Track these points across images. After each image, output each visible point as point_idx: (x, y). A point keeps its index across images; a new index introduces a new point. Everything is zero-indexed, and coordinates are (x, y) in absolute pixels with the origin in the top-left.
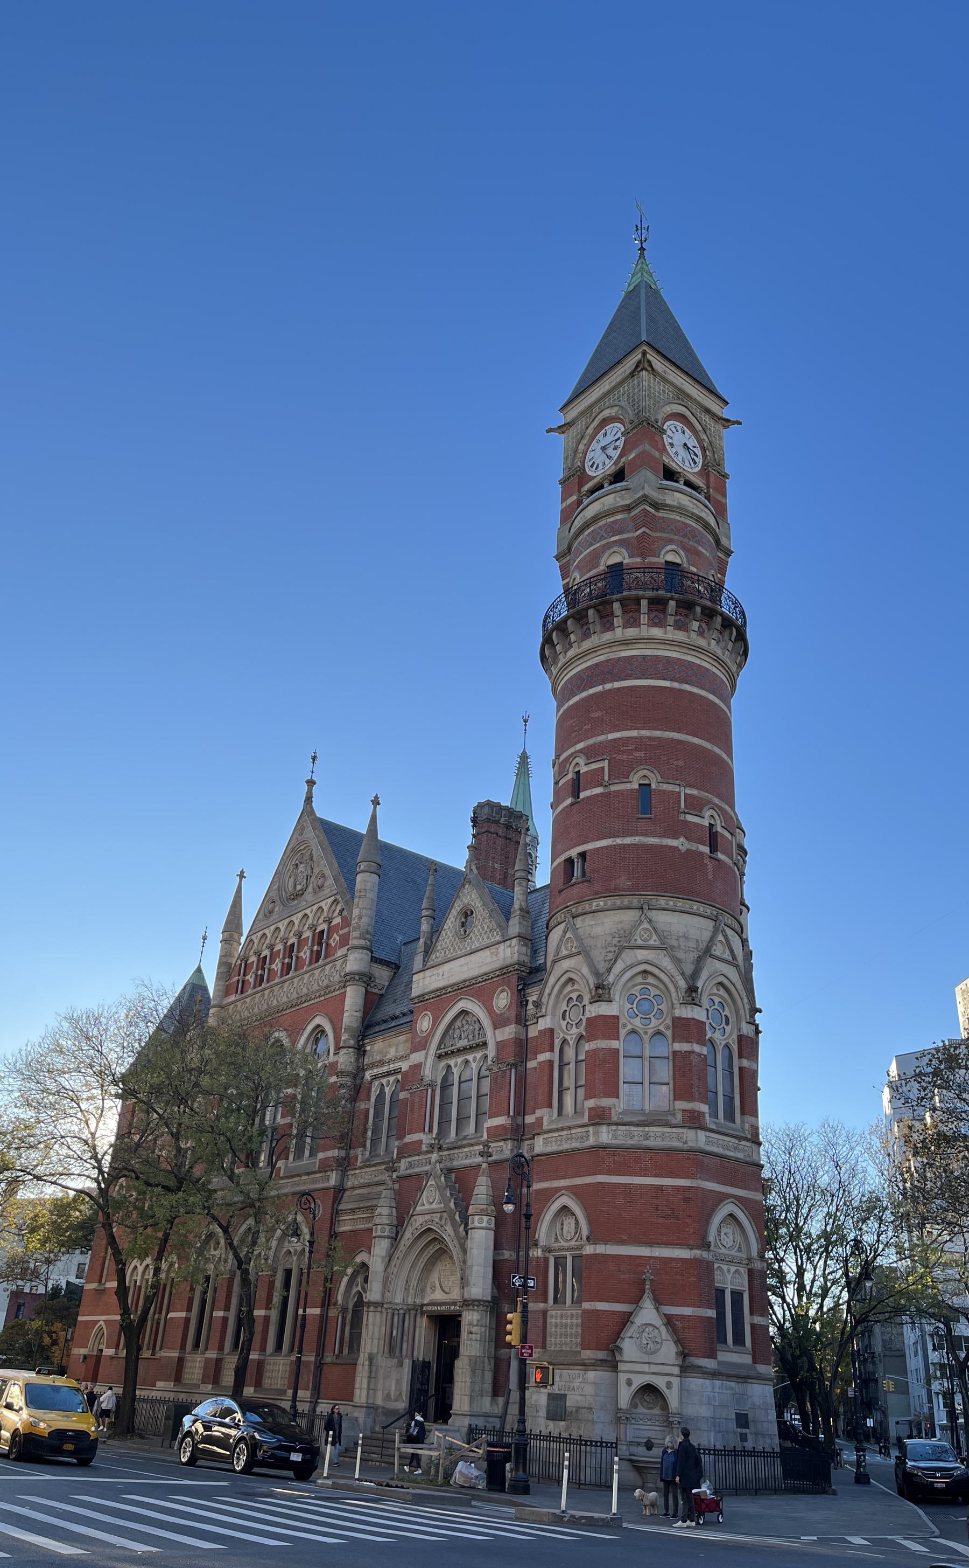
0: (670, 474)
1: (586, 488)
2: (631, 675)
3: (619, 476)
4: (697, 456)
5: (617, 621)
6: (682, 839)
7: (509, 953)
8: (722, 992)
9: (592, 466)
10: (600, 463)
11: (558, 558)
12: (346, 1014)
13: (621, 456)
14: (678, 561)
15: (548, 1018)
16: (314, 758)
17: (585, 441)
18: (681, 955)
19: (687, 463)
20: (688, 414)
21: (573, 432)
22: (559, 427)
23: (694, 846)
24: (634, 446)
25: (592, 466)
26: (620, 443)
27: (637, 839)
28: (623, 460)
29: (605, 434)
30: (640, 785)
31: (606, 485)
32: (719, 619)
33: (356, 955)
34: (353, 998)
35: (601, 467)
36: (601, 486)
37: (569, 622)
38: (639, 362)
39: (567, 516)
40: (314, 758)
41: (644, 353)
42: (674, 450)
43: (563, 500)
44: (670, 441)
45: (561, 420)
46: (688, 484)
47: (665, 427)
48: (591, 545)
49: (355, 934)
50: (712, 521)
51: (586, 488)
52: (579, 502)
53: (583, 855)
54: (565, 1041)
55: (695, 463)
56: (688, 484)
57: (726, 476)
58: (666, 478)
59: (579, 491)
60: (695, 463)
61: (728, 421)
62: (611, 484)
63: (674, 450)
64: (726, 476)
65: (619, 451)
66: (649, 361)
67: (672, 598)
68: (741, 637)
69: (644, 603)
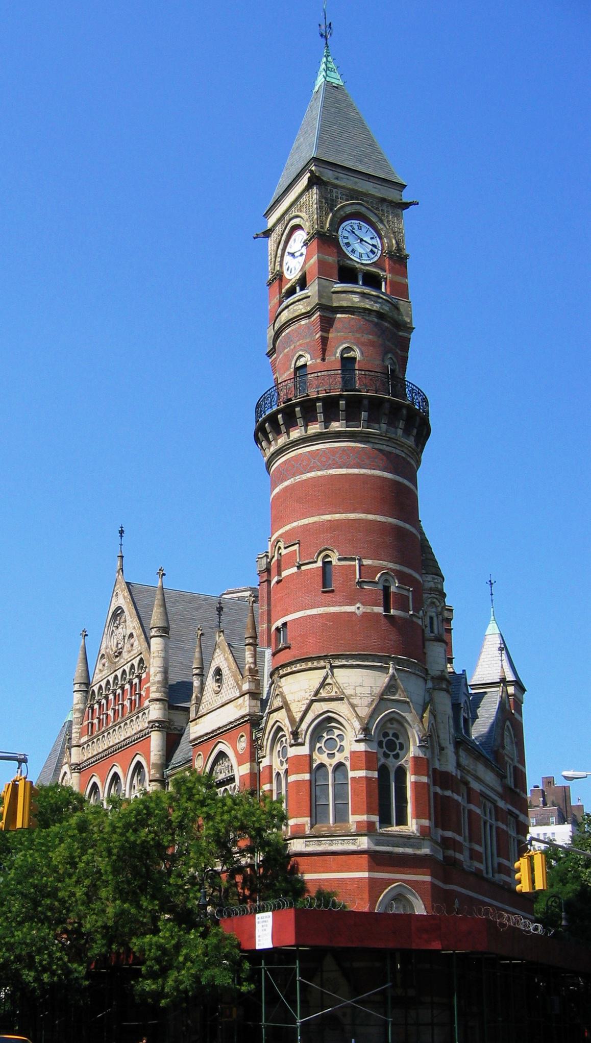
2: (314, 467)
6: (358, 605)
7: (244, 707)
8: (395, 725)
12: (152, 754)
13: (305, 263)
15: (268, 757)
16: (121, 532)
17: (281, 246)
18: (355, 701)
20: (363, 210)
23: (368, 609)
27: (322, 609)
30: (324, 563)
31: (298, 288)
33: (155, 706)
34: (156, 740)
40: (121, 532)
44: (346, 241)
49: (153, 689)
53: (285, 625)
54: (278, 774)
58: (342, 281)
59: (280, 292)
63: (350, 249)
65: (304, 257)
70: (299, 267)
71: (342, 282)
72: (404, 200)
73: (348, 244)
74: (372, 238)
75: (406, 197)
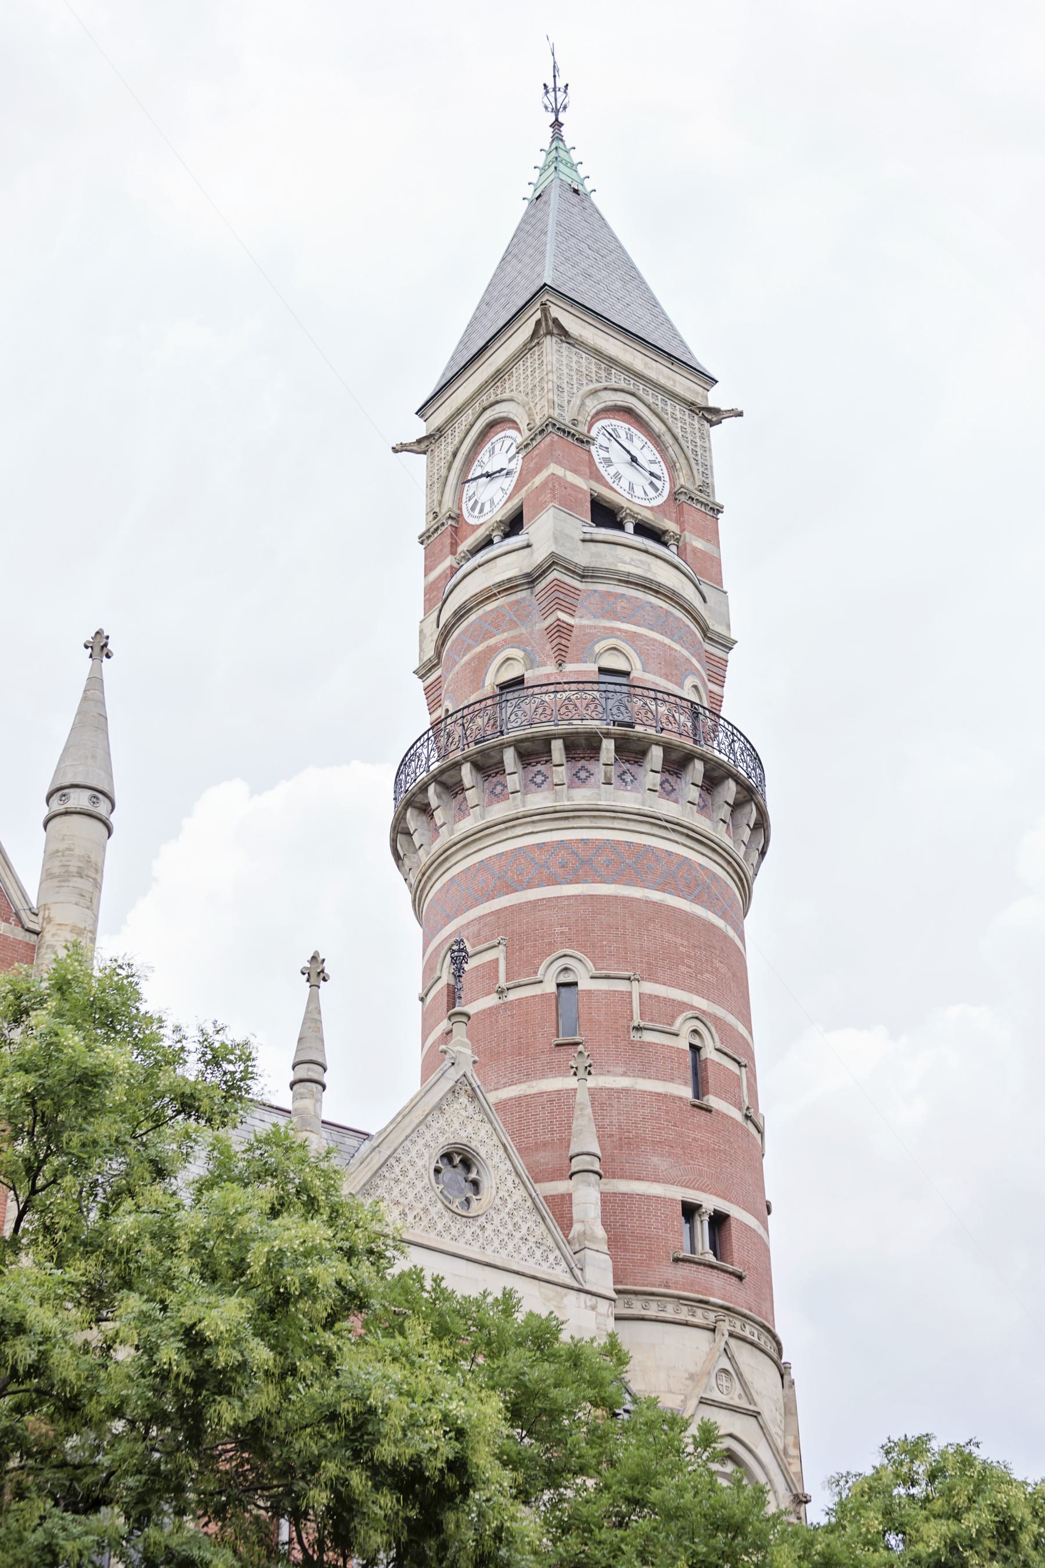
0: (605, 514)
1: (465, 546)
3: (514, 524)
4: (658, 478)
5: (513, 782)
9: (473, 509)
10: (488, 502)
11: (423, 672)
13: (518, 487)
14: (620, 664)
19: (638, 492)
21: (444, 449)
22: (419, 441)
24: (538, 470)
25: (473, 509)
26: (516, 465)
28: (523, 493)
29: (492, 451)
32: (699, 766)
35: (487, 508)
36: (489, 542)
37: (431, 789)
38: (538, 323)
39: (435, 595)
41: (545, 310)
42: (612, 470)
43: (428, 570)
45: (420, 429)
46: (643, 529)
47: (593, 433)
48: (469, 648)
50: (689, 592)
51: (465, 546)
52: (454, 571)
55: (656, 489)
56: (643, 529)
57: (717, 510)
60: (656, 489)
61: (715, 411)
62: (506, 535)
63: (612, 470)
64: (717, 510)
66: (555, 321)
67: (607, 735)
68: (750, 795)
69: (557, 746)
70: (500, 498)
71: (598, 526)
72: (712, 404)
73: (608, 462)
74: (652, 462)
75: (715, 398)
